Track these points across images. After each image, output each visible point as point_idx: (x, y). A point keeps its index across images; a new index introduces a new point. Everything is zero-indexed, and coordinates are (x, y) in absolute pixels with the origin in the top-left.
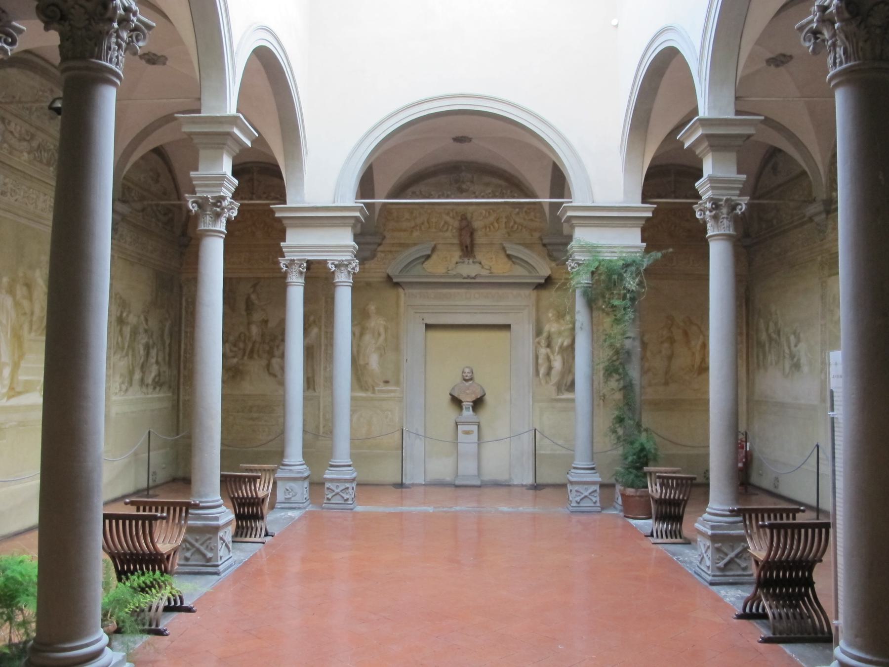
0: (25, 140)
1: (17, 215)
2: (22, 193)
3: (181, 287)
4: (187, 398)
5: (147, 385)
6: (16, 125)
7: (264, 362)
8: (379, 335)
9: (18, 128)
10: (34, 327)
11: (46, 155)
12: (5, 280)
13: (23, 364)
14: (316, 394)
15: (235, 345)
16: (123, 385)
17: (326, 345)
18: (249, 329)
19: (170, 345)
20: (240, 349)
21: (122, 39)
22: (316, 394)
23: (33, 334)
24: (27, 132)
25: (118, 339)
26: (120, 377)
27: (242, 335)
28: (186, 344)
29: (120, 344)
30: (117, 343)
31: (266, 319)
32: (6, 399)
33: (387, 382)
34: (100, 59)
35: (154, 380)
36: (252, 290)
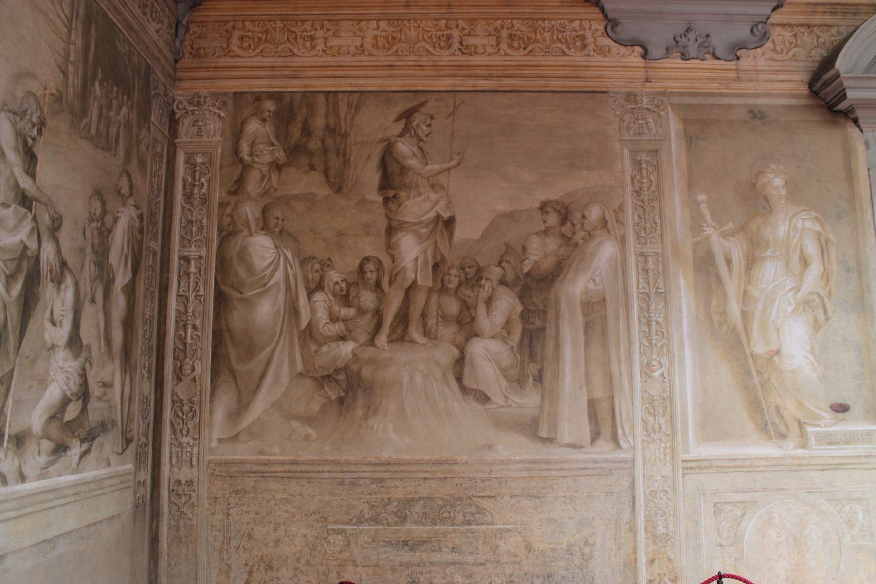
3: (173, 122)
4: (185, 474)
5: (20, 440)
7: (446, 354)
8: (805, 262)
14: (620, 455)
15: (346, 299)
17: (646, 297)
18: (390, 248)
19: (130, 290)
20: (361, 312)
22: (620, 455)
27: (370, 266)
28: (183, 298)
31: (446, 215)
33: (841, 409)
35: (55, 416)
36: (400, 127)
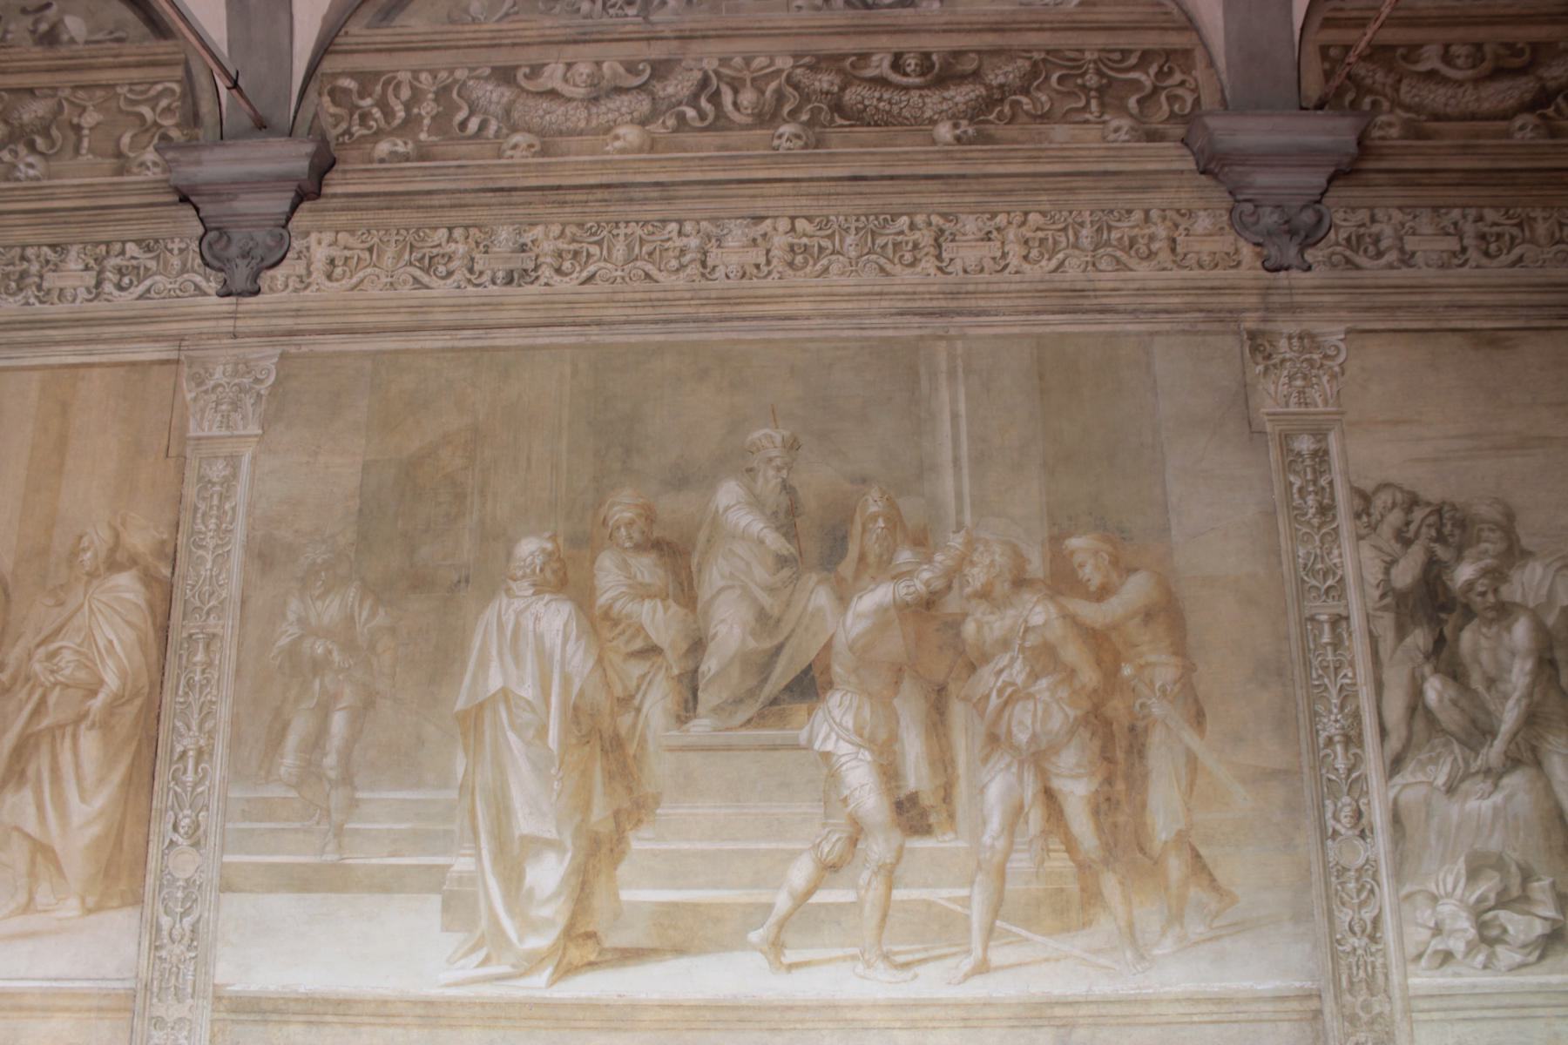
0: (620, 90)
1: (599, 324)
2: (619, 251)
6: (569, 65)
9: (584, 69)
10: (707, 699)
11: (748, 97)
12: (529, 548)
13: (639, 843)
16: (1503, 915)
23: (701, 727)
24: (631, 68)
25: (1417, 692)
26: (1473, 874)
29: (1450, 718)
30: (1416, 705)
32: (548, 972)
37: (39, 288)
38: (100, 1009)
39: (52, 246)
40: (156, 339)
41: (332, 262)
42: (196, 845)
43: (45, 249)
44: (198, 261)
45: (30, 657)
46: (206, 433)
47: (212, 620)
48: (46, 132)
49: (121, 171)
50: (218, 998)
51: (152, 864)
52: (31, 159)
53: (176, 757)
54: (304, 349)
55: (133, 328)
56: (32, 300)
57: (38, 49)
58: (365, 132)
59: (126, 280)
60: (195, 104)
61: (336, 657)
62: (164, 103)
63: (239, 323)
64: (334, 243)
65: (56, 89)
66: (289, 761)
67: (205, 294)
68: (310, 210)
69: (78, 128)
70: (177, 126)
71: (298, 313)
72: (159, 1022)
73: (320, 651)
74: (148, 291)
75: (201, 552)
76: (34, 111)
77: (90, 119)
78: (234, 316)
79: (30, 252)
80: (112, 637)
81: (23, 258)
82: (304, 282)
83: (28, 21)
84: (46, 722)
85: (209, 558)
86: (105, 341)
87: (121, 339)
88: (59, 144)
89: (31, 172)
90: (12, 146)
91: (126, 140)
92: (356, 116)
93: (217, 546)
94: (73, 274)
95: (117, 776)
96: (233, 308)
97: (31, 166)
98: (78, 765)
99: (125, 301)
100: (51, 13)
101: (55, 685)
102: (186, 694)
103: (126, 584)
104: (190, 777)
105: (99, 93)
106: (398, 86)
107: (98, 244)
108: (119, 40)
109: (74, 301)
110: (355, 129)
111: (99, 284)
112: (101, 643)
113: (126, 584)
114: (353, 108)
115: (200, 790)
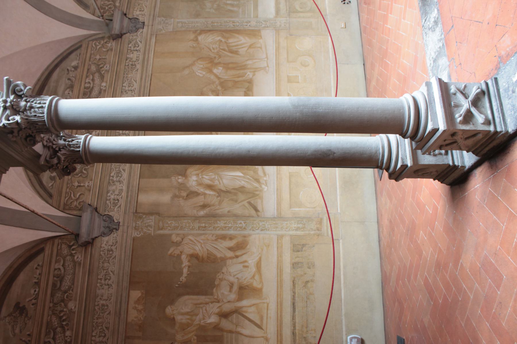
21: (26, 106)
34: (45, 120)
37: (135, 61)
38: (278, 35)
39: (126, 60)
40: (151, 39)
41: (140, 11)
42: (250, 22)
43: (127, 62)
44: (135, 33)
45: (213, 53)
46: (172, 28)
47: (209, 23)
48: (99, 65)
49: (112, 50)
50: (276, 17)
51: (253, 28)
52: (105, 67)
53: (233, 26)
54: (157, 14)
55: (148, 43)
56: (138, 62)
57: (78, 70)
58: (113, 8)
59: (137, 46)
60: (99, 38)
61: (217, 3)
62: (97, 44)
63: (150, 24)
64: (136, 11)
65: (89, 65)
66: (235, 9)
67: (143, 31)
68: (129, 14)
69: (100, 59)
70: (104, 40)
71: (150, 15)
72: (280, 26)
73: (216, 6)
74: (140, 41)
75: (196, 26)
76: (93, 68)
77: (98, 57)
78: (148, 26)
79: (127, 64)
80: (211, 39)
81: (128, 65)
82: (142, 15)
83: (70, 72)
84: (227, 49)
85: (197, 24)
86: (149, 48)
87: (150, 45)
88: (102, 62)
89: (108, 67)
90: (101, 71)
91: (104, 50)
92: (110, 9)
93: (195, 23)
94: (133, 56)
95: (237, 35)
96: (147, 26)
97: (107, 67)
98: (235, 42)
99: (141, 46)
100: (69, 68)
101: (219, 47)
102: (222, 26)
103: (200, 38)
104: (238, 24)
105: (92, 56)
106: (104, 3)
107: (128, 51)
108: (80, 54)
109: (140, 55)
110: (112, 9)
111: (137, 50)
112: (212, 40)
113: (200, 38)
114: (108, 10)
115: (240, 22)
